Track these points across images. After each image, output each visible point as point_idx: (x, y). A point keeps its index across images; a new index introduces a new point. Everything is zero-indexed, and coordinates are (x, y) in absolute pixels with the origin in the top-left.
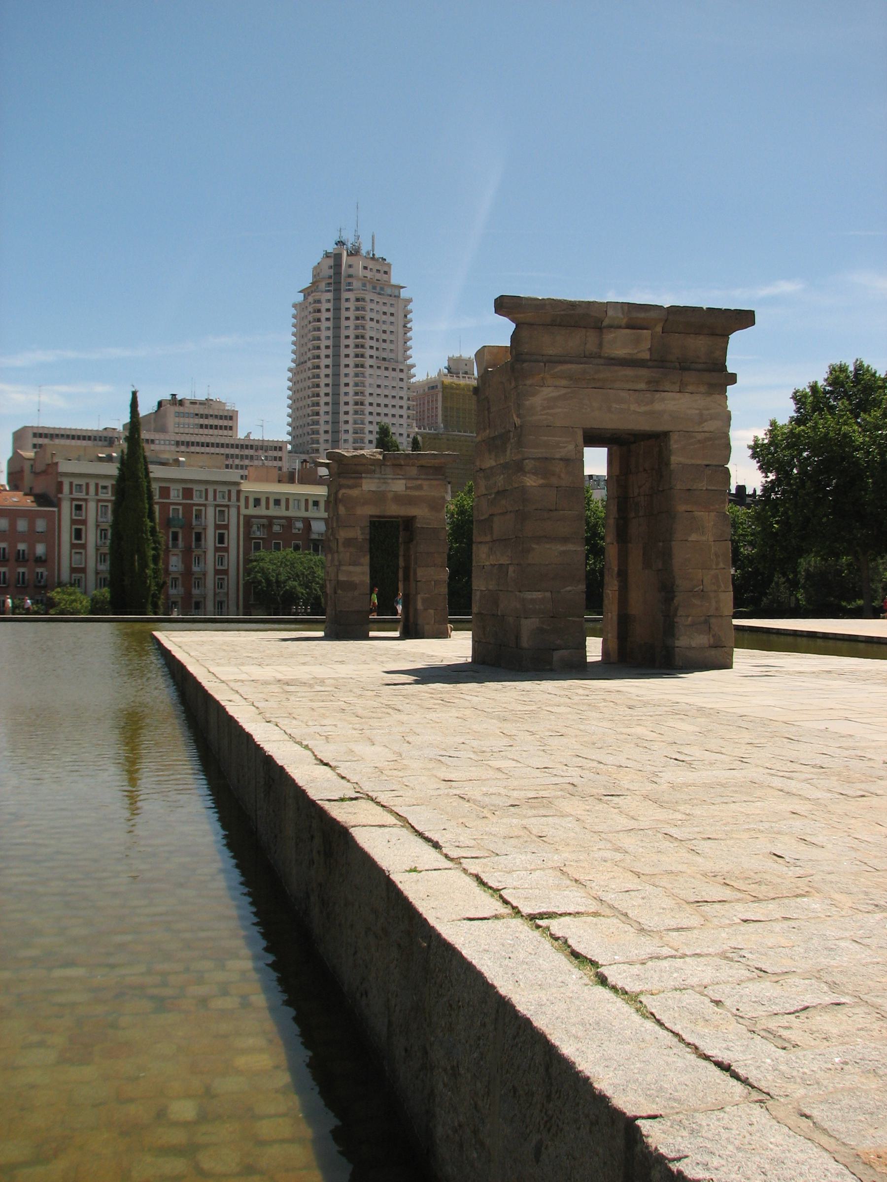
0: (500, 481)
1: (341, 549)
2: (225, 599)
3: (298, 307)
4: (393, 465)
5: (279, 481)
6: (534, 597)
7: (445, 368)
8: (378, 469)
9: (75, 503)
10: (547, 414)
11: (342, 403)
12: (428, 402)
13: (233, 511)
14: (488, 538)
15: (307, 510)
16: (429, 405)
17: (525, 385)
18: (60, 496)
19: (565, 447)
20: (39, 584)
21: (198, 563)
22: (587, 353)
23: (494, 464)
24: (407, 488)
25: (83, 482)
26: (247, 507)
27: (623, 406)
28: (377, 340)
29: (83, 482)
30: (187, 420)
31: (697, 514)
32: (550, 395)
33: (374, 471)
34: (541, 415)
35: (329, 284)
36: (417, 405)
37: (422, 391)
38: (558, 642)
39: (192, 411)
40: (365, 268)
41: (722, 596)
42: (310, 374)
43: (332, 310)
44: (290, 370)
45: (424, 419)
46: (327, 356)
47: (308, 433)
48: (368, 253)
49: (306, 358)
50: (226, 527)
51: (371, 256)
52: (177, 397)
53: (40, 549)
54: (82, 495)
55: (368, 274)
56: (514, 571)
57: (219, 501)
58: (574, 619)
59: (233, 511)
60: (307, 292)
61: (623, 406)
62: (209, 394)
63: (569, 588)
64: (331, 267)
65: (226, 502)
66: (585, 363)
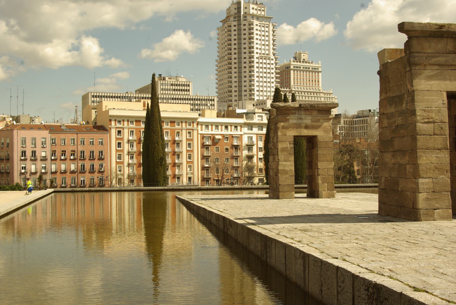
0: (399, 121)
1: (279, 153)
2: (192, 176)
3: (220, 30)
4: (304, 110)
5: (217, 117)
6: (424, 181)
7: (294, 58)
8: (297, 112)
10: (428, 84)
11: (243, 77)
12: (285, 75)
14: (391, 149)
15: (231, 131)
16: (286, 77)
17: (416, 69)
19: (437, 102)
20: (100, 170)
21: (178, 158)
22: (447, 52)
23: (394, 111)
24: (312, 121)
26: (202, 130)
32: (429, 74)
33: (295, 113)
34: (424, 85)
35: (235, 17)
36: (281, 76)
37: (282, 70)
40: (253, 8)
42: (226, 62)
43: (237, 30)
45: (283, 83)
46: (235, 54)
47: (226, 92)
49: (224, 55)
50: (192, 140)
54: (121, 126)
55: (255, 12)
56: (411, 168)
57: (188, 127)
58: (445, 193)
59: (195, 132)
60: (224, 22)
62: (177, 74)
63: (442, 176)
64: (235, 9)
65: (191, 127)
66: (446, 57)
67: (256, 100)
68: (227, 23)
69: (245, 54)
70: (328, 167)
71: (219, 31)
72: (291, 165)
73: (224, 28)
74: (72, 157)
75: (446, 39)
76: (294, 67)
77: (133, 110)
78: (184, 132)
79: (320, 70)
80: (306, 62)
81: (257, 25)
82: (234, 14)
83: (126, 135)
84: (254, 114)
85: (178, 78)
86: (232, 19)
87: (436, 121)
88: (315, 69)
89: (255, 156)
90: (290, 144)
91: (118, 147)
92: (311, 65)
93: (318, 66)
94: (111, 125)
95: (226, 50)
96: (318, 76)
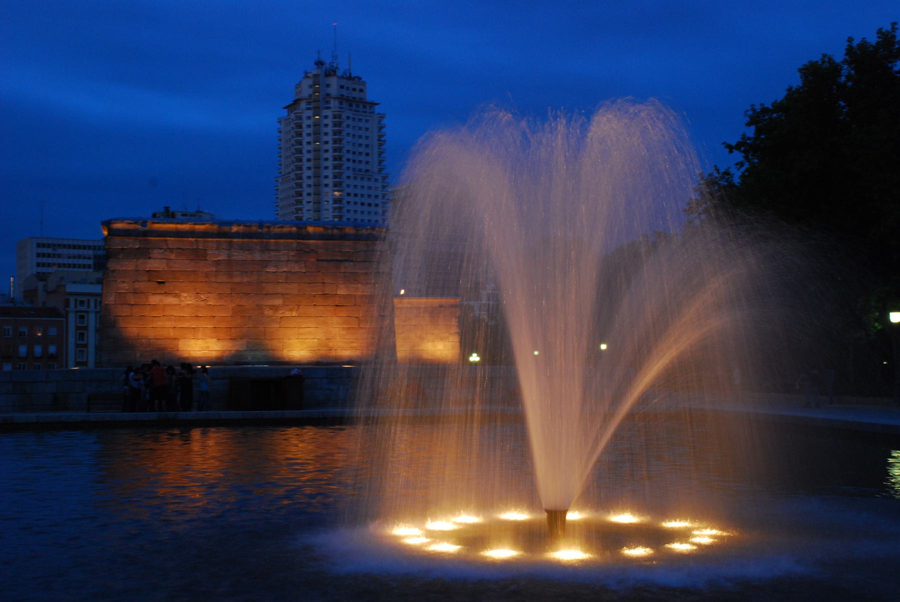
9: (79, 314)
18: (67, 309)
25: (85, 299)
28: (354, 153)
29: (85, 299)
48: (345, 73)
49: (290, 169)
51: (348, 75)
52: (170, 209)
53: (52, 349)
54: (85, 308)
68: (295, 112)
69: (326, 171)
71: (281, 124)
73: (290, 120)
82: (307, 95)
85: (200, 214)
86: (303, 105)
91: (79, 340)
95: (293, 161)
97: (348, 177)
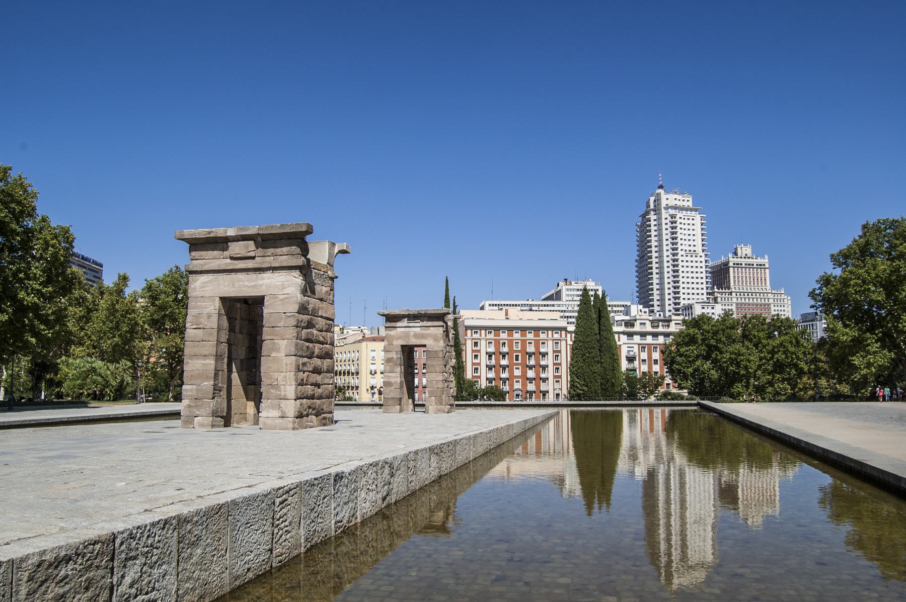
2: (560, 392)
9: (473, 341)
13: (563, 343)
27: (242, 283)
30: (572, 293)
31: (276, 341)
38: (197, 413)
39: (575, 287)
41: (288, 388)
44: (636, 261)
59: (563, 343)
61: (242, 283)
63: (205, 383)
67: (681, 304)
70: (436, 379)
72: (397, 377)
74: (424, 371)
75: (221, 244)
76: (734, 264)
77: (493, 319)
78: (550, 343)
79: (767, 266)
80: (749, 258)
81: (680, 218)
83: (483, 347)
84: (636, 320)
87: (206, 327)
88: (760, 265)
89: (638, 370)
90: (396, 354)
92: (755, 260)
93: (764, 261)
94: (466, 335)
96: (765, 273)
97: (682, 256)
